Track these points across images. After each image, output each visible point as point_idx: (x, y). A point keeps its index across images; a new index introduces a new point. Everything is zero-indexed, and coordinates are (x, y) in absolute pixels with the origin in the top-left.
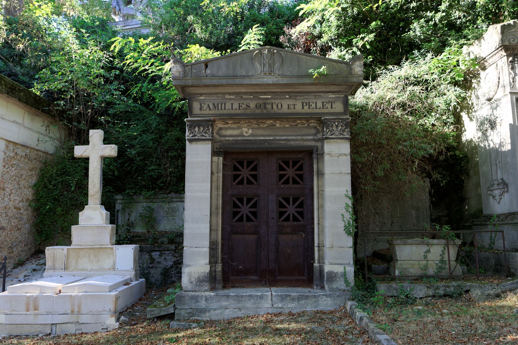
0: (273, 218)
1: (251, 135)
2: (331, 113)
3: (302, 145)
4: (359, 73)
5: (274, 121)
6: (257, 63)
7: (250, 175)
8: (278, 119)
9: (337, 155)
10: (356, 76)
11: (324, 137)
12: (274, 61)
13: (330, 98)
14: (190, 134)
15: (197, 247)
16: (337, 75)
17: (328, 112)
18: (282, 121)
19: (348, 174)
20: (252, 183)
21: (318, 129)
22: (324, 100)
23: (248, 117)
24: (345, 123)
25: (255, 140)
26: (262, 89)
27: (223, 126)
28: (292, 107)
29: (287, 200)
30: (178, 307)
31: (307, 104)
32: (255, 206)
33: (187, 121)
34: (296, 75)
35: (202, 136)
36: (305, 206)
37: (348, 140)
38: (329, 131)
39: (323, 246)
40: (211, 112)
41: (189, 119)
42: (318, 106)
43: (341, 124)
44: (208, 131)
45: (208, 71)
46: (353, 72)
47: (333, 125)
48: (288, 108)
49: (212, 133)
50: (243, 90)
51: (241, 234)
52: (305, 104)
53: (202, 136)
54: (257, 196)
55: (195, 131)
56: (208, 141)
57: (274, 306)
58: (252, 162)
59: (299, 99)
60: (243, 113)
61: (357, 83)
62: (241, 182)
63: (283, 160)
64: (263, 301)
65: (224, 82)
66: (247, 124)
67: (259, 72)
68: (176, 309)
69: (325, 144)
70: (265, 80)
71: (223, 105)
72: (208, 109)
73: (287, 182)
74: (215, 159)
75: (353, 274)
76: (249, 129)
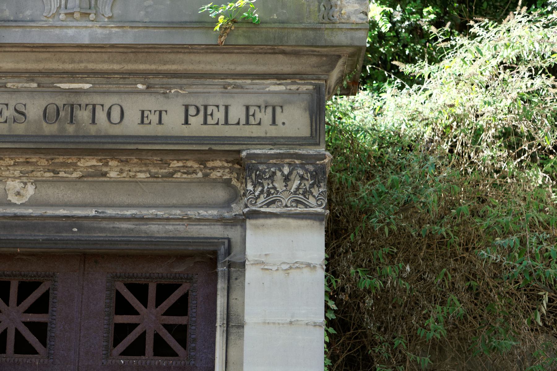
2: (272, 138)
3: (182, 235)
4: (354, 19)
5: (100, 160)
7: (26, 324)
8: (113, 153)
10: (344, 26)
13: (270, 92)
16: (287, 22)
17: (263, 135)
18: (127, 161)
19: (315, 325)
20: (33, 351)
21: (234, 188)
22: (252, 100)
24: (311, 168)
25: (41, 217)
26: (64, 62)
28: (154, 118)
31: (198, 111)
34: (163, 20)
37: (321, 220)
38: (262, 192)
42: (232, 119)
43: (301, 172)
46: (336, 15)
47: (274, 173)
48: (142, 122)
52: (192, 111)
58: (36, 285)
59: (177, 94)
60: (5, 133)
61: (350, 50)
63: (129, 281)
66: (19, 168)
67: (54, 10)
69: (249, 233)
70: (70, 32)
76: (25, 184)
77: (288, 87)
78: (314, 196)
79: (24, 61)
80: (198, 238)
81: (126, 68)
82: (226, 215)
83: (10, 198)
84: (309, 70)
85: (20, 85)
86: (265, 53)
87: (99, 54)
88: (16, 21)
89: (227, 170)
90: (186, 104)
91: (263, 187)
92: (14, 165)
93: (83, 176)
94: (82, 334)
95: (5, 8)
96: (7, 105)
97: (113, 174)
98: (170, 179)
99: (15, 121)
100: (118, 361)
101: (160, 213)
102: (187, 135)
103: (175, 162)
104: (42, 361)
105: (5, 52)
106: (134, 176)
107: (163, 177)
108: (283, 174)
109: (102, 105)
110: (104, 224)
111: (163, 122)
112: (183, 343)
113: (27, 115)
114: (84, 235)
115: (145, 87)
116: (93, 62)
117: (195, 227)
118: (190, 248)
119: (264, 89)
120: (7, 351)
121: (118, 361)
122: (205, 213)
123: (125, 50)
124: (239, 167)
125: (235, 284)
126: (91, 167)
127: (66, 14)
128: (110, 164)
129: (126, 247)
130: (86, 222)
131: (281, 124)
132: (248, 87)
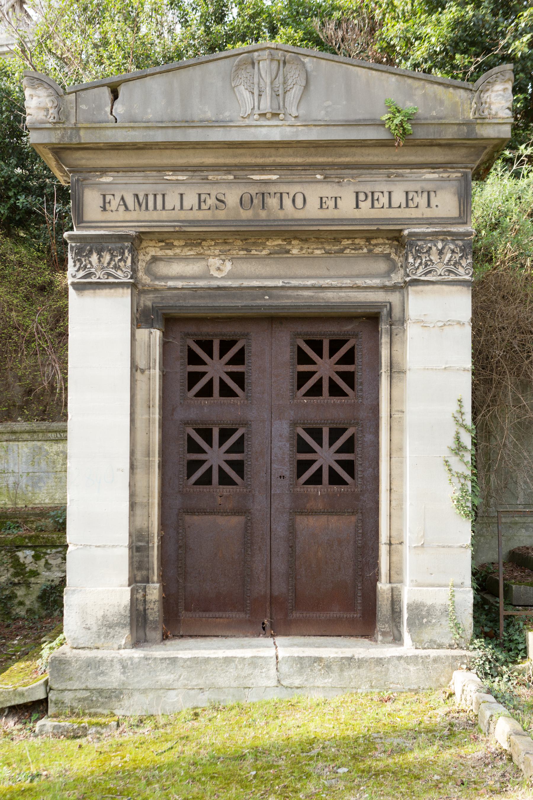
0: (282, 477)
1: (230, 276)
2: (427, 219)
3: (353, 300)
5: (285, 240)
6: (242, 88)
7: (227, 373)
9: (442, 324)
11: (408, 279)
12: (285, 83)
14: (78, 270)
15: (99, 547)
19: (464, 370)
20: (235, 395)
21: (393, 261)
22: (411, 187)
23: (221, 229)
24: (460, 243)
26: (256, 157)
27: (160, 253)
28: (331, 203)
29: (316, 434)
30: (54, 686)
31: (366, 196)
32: (238, 447)
33: (71, 238)
35: (109, 275)
36: (358, 449)
38: (421, 264)
39: (401, 543)
40: (129, 216)
41: (76, 232)
42: (395, 204)
43: (452, 247)
44: (122, 264)
45: (119, 108)
47: (430, 248)
48: (321, 207)
49: (134, 270)
50: (209, 159)
51: (204, 512)
52: (362, 197)
53: (109, 275)
54: (245, 424)
55: (90, 263)
56: (123, 288)
57: (282, 682)
58: (233, 343)
60: (210, 218)
61: (496, 142)
62: (207, 392)
63: (308, 338)
64: (257, 672)
65: (159, 136)
67: (249, 112)
68: (50, 689)
69: (411, 297)
70: (264, 130)
71: (159, 198)
72: (122, 208)
73: (316, 391)
74: (142, 333)
75: (470, 610)
76: (224, 261)
77: (441, 175)
78: (463, 267)
79: (223, 156)
80: (366, 302)
81: (307, 161)
82: (387, 283)
83: (212, 273)
84: (459, 159)
85: (219, 177)
86: (425, 146)
87: (286, 149)
88: (217, 121)
89: (387, 246)
90: (357, 191)
91: (422, 260)
92: (215, 245)
93: (270, 254)
94: (273, 380)
95: (207, 109)
96: (209, 194)
97: (295, 251)
98: (341, 255)
99: (217, 208)
100: (302, 401)
101: (335, 283)
102: (358, 217)
103: (346, 240)
104: (242, 402)
105: (207, 148)
106: (312, 253)
107: (335, 253)
108: (438, 250)
109: (288, 193)
110: (289, 293)
111: (338, 206)
112: (352, 386)
113: (227, 203)
114: (275, 302)
115: (322, 177)
116: (280, 156)
117: (362, 293)
118: (359, 311)
119: (420, 177)
120: (214, 395)
121: (302, 401)
122: (370, 282)
123: (308, 145)
124: (397, 243)
125: (396, 339)
126: (277, 245)
127: (259, 115)
128: (293, 242)
129: (308, 310)
130: (275, 292)
131: (434, 207)
132: (407, 175)
